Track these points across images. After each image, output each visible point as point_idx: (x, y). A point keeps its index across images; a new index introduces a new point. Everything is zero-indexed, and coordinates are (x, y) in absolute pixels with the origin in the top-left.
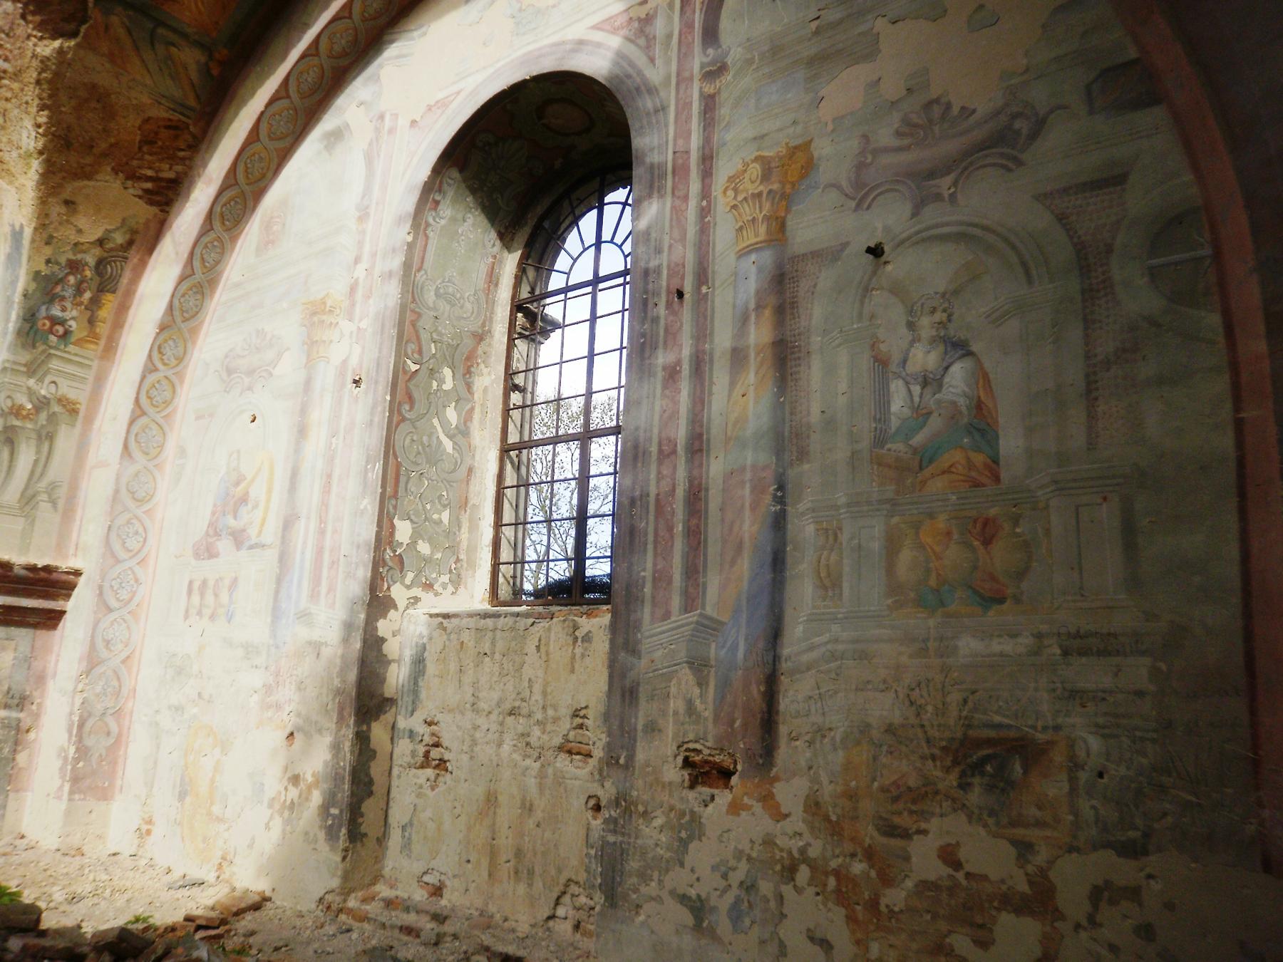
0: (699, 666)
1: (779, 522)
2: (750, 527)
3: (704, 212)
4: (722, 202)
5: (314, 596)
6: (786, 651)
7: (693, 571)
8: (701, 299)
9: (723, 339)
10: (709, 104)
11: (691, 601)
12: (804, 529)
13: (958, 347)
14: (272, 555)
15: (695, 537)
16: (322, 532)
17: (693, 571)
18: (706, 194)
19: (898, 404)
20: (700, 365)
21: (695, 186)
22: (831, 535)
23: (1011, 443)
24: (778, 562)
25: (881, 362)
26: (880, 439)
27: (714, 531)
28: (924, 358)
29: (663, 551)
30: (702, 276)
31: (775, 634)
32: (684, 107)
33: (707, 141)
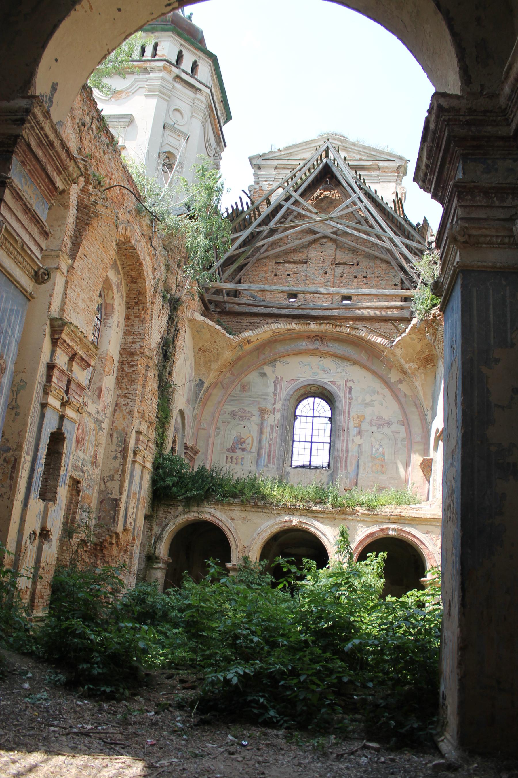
0: (347, 478)
1: (358, 462)
2: (355, 462)
3: (348, 420)
4: (351, 419)
5: (269, 462)
6: (359, 477)
7: (346, 466)
8: (348, 432)
9: (351, 438)
10: (350, 403)
11: (345, 470)
12: (361, 463)
13: (381, 446)
14: (255, 455)
15: (346, 462)
16: (270, 452)
17: (346, 466)
18: (349, 417)
19: (374, 451)
20: (347, 441)
21: (347, 415)
22: (365, 464)
23: (386, 458)
24: (358, 466)
25: (372, 446)
26: (371, 455)
27: (349, 462)
28: (377, 446)
29: (342, 463)
30: (348, 429)
31: (357, 475)
32: (345, 402)
33: (349, 409)
